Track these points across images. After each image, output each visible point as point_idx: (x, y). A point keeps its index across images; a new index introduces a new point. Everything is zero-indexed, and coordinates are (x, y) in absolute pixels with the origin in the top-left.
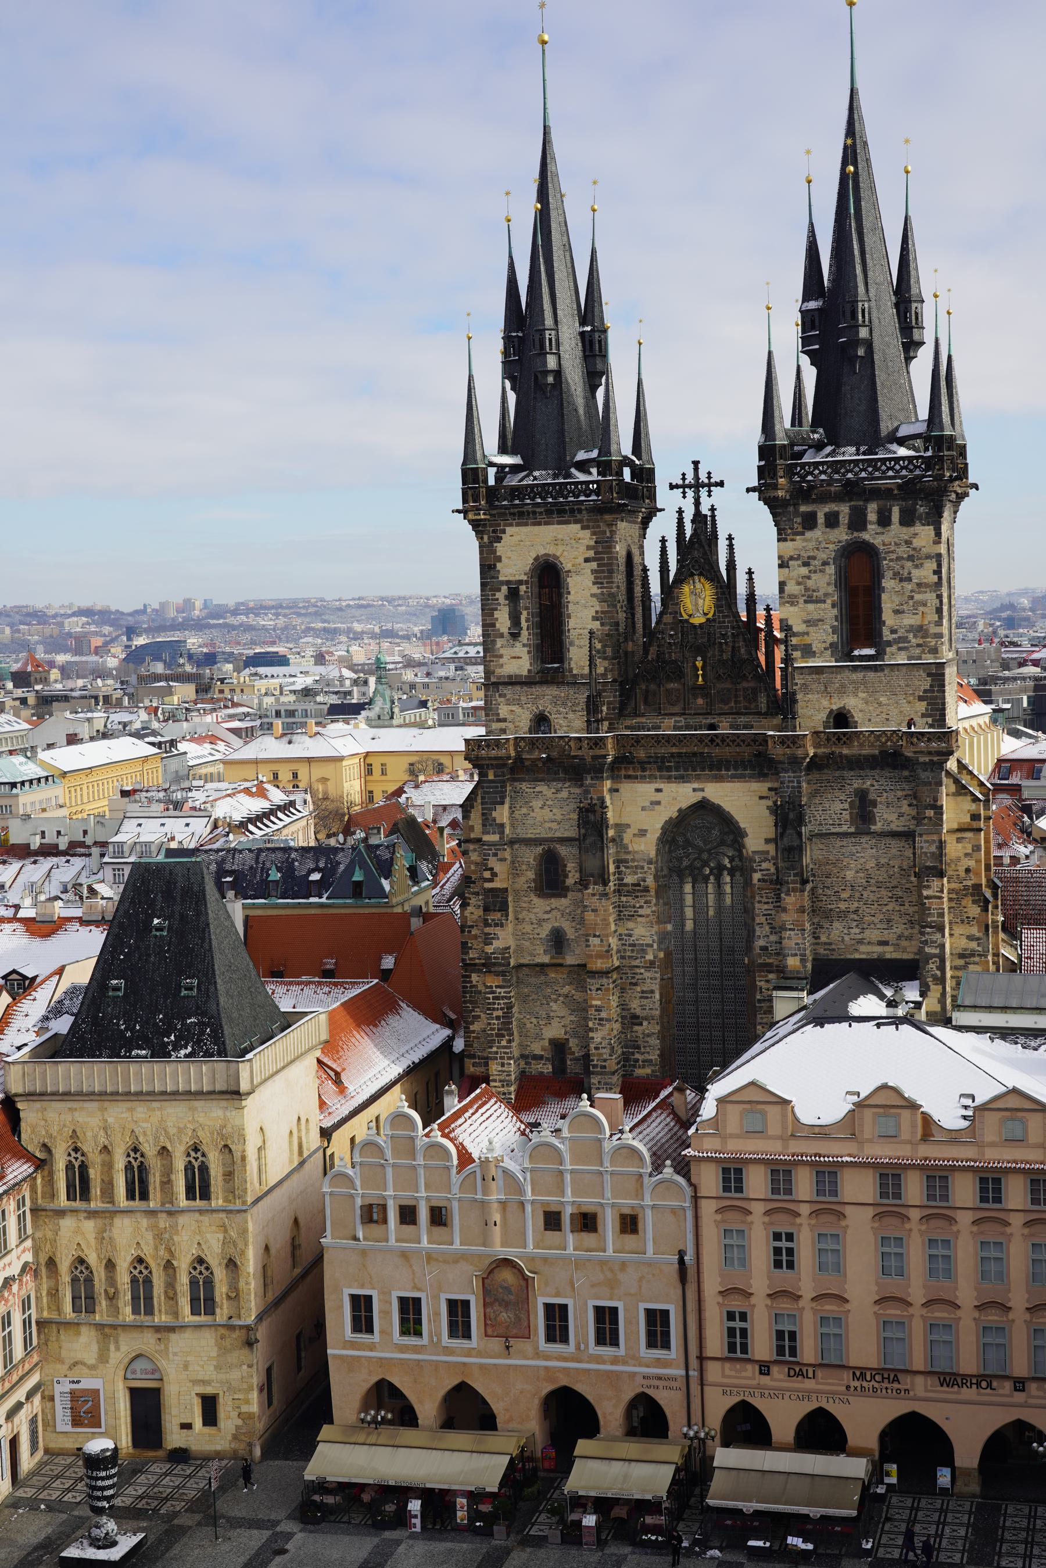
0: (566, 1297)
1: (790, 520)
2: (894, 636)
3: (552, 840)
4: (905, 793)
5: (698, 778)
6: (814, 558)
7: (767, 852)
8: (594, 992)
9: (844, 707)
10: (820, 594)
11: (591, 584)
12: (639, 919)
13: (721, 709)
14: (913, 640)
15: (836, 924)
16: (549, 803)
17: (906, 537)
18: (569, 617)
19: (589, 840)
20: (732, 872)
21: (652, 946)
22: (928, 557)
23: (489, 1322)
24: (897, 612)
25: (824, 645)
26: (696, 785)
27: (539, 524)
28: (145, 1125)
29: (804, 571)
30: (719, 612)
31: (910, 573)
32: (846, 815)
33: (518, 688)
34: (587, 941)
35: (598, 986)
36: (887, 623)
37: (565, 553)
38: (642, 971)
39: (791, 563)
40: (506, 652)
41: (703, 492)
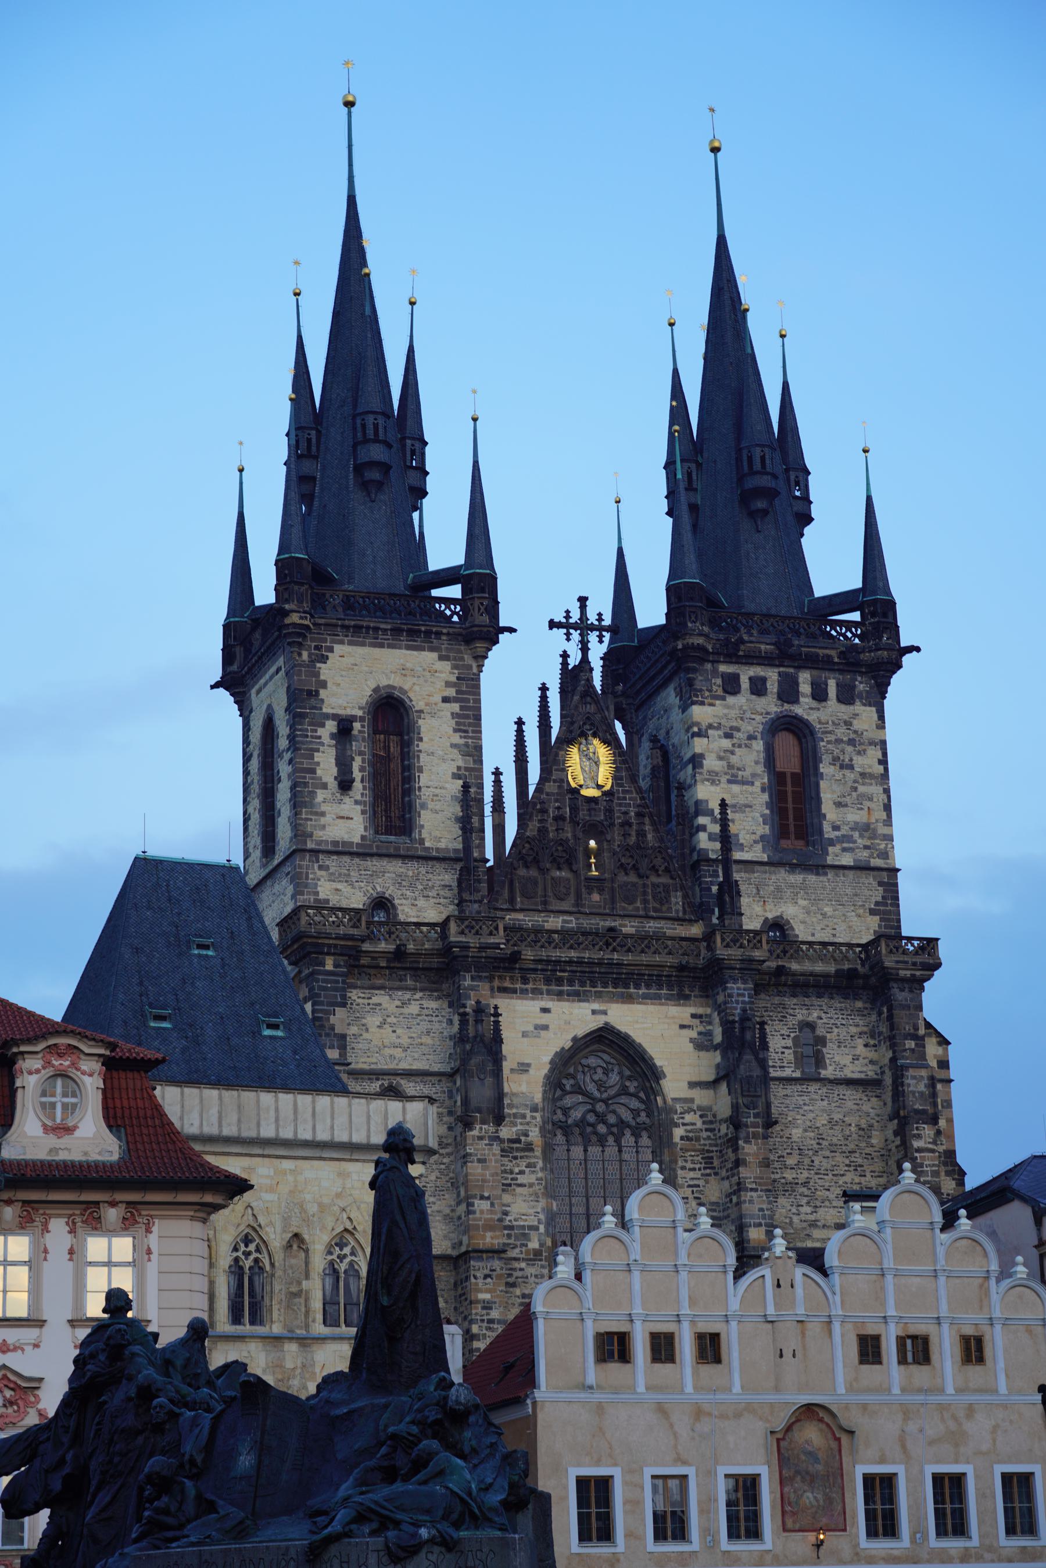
0: (894, 1462)
1: (708, 680)
2: (837, 833)
3: (395, 1073)
4: (859, 1029)
5: (599, 996)
6: (738, 730)
7: (692, 1100)
8: (480, 1281)
9: (781, 917)
10: (747, 774)
12: (519, 1190)
13: (624, 909)
14: (859, 841)
15: (782, 1201)
17: (846, 717)
18: (421, 770)
19: (475, 1061)
20: (637, 1136)
21: (537, 1228)
22: (872, 743)
23: (788, 1508)
24: (839, 805)
25: (753, 837)
26: (596, 1006)
27: (382, 646)
28: (267, 1197)
29: (726, 743)
30: (619, 785)
31: (851, 760)
32: (789, 1055)
33: (346, 859)
34: (470, 1205)
35: (487, 1272)
36: (828, 817)
37: (417, 688)
38: (523, 1265)
39: (710, 732)
40: (331, 810)
41: (593, 637)
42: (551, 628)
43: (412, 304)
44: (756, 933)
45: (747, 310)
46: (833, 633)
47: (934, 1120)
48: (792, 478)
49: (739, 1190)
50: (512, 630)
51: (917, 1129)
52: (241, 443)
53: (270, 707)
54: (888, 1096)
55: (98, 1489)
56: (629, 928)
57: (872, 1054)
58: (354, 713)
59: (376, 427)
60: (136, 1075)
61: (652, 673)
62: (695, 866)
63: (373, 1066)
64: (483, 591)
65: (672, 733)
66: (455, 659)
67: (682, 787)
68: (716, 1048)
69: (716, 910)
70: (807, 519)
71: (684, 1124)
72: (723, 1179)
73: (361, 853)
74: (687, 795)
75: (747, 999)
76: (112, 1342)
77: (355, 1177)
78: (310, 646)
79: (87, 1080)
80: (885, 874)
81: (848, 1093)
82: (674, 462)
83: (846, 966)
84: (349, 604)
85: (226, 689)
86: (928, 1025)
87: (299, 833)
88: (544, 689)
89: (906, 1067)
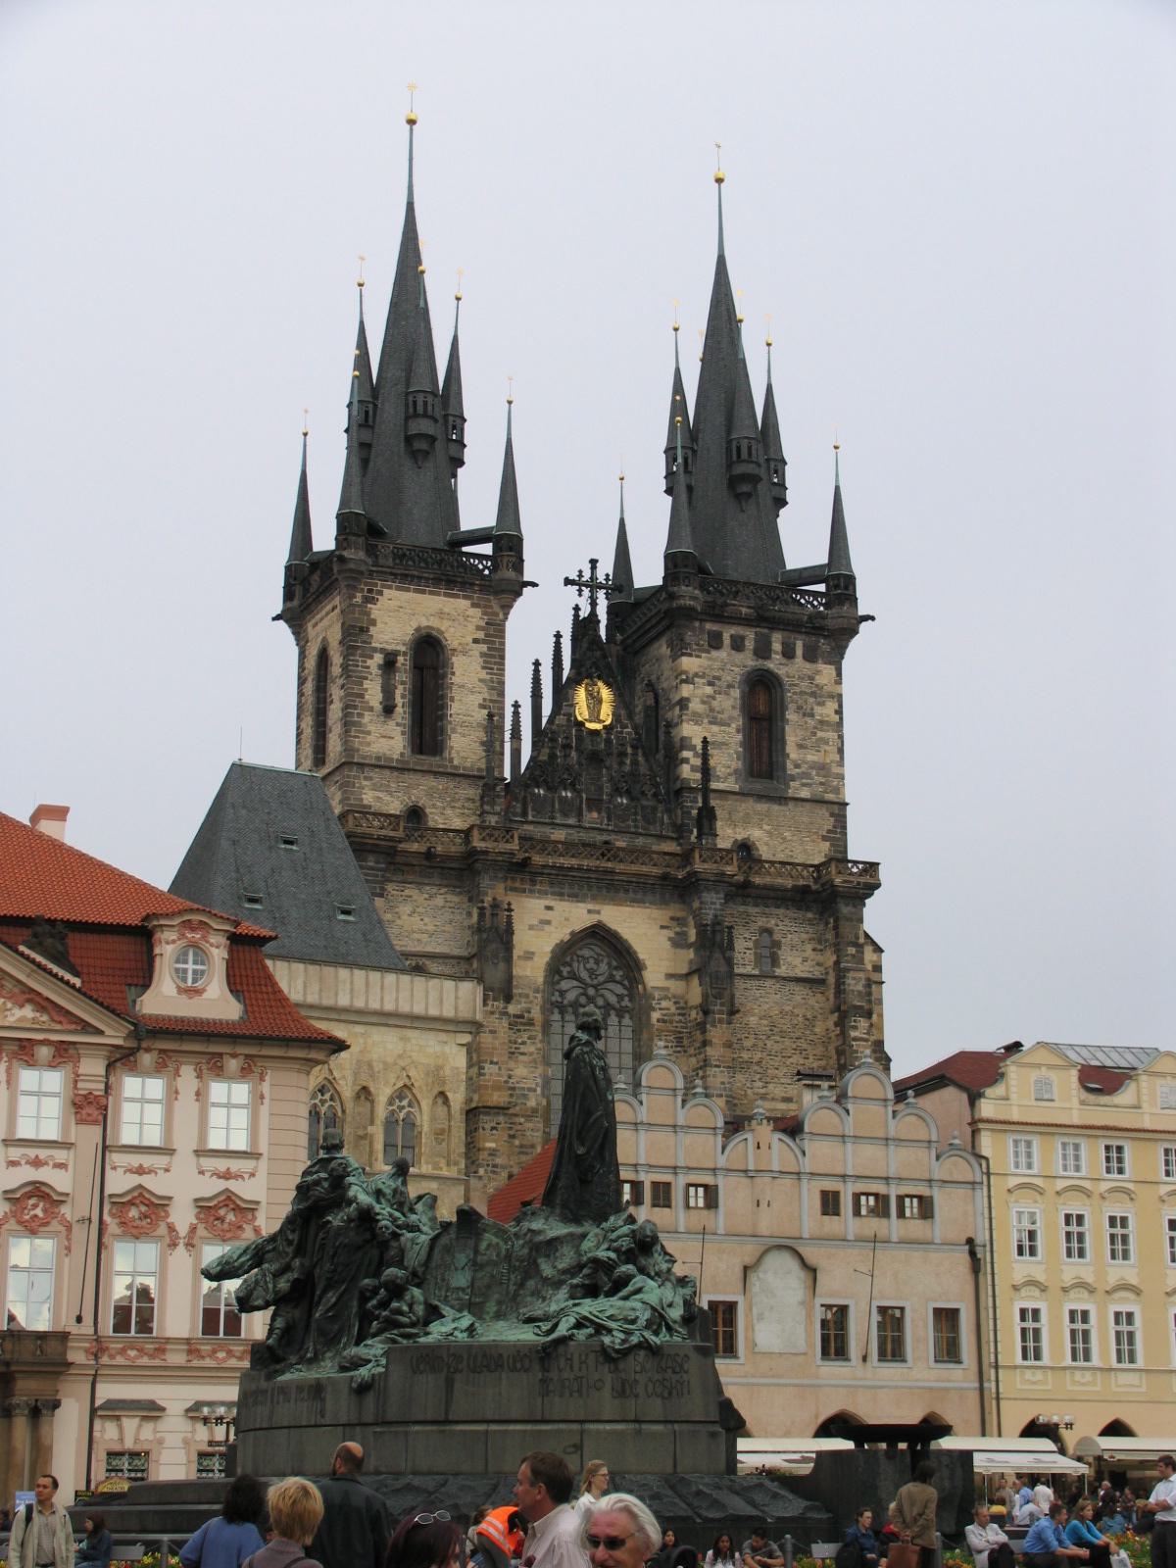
5: (594, 898)
7: (667, 989)
8: (488, 1131)
9: (748, 839)
10: (725, 716)
11: (479, 669)
12: (521, 1057)
16: (420, 910)
20: (620, 1016)
21: (535, 1090)
22: (831, 696)
24: (800, 746)
25: (728, 771)
26: (591, 906)
29: (709, 690)
31: (812, 709)
32: (750, 955)
33: (387, 772)
35: (493, 1124)
38: (522, 1120)
42: (566, 585)
43: (458, 299)
44: (728, 851)
45: (741, 321)
46: (803, 601)
47: (869, 1014)
48: (772, 466)
49: (705, 1066)
50: (534, 585)
51: (855, 1021)
52: (306, 411)
53: (324, 639)
54: (831, 993)
55: (324, 1292)
56: (621, 843)
57: (820, 958)
58: (398, 648)
59: (425, 403)
60: (252, 949)
61: (648, 626)
62: (678, 792)
63: (403, 948)
64: (511, 549)
65: (663, 678)
66: (485, 607)
67: (669, 725)
68: (689, 946)
69: (695, 831)
70: (782, 502)
71: (660, 1009)
72: (691, 1056)
73: (401, 768)
74: (674, 732)
75: (718, 906)
76: (335, 1174)
77: (414, 1041)
78: (362, 590)
79: (215, 951)
80: (836, 807)
81: (797, 988)
82: (675, 448)
83: (801, 882)
84: (400, 556)
85: (286, 622)
86: (867, 936)
87: (348, 749)
88: (558, 636)
89: (848, 970)
